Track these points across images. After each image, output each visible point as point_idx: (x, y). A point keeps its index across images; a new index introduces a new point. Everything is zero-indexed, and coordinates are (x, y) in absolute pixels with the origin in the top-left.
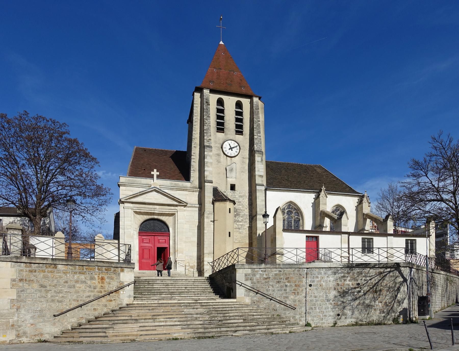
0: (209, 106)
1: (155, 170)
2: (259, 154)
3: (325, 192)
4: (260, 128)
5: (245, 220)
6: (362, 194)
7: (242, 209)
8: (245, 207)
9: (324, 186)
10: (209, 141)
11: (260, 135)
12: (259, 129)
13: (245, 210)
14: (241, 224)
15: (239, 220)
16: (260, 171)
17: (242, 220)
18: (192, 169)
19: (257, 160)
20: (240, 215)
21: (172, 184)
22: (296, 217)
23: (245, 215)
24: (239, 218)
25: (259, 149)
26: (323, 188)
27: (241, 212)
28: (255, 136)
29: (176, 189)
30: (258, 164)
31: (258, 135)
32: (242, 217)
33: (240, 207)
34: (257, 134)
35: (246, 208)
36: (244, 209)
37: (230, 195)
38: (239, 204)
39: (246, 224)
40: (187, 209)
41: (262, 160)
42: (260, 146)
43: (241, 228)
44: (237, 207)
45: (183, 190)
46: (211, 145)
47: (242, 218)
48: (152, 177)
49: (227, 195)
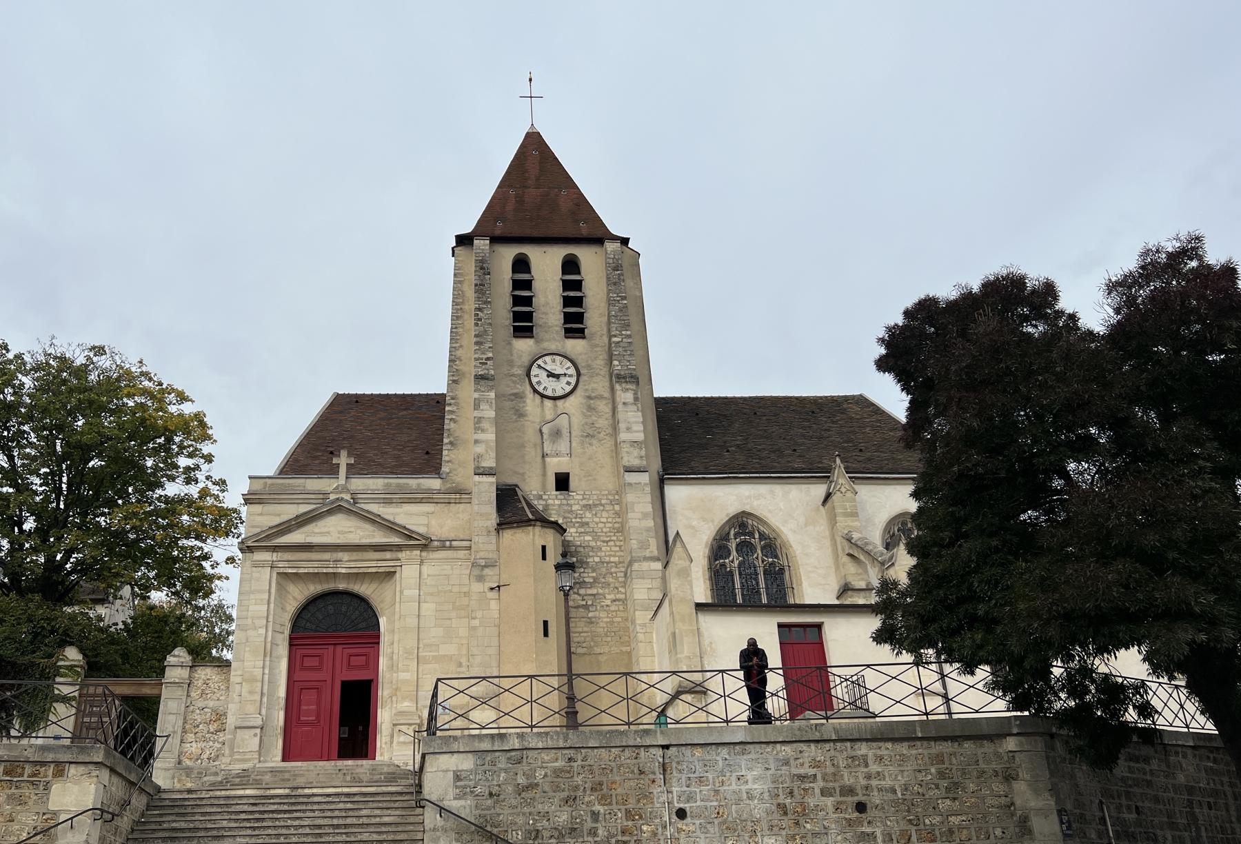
1: (344, 453)
2: (626, 382)
3: (847, 475)
5: (603, 580)
8: (602, 538)
11: (629, 333)
13: (603, 549)
14: (594, 591)
15: (587, 580)
17: (596, 580)
19: (623, 400)
20: (587, 563)
21: (388, 485)
22: (770, 560)
23: (603, 563)
24: (586, 575)
27: (591, 554)
28: (615, 336)
29: (400, 498)
30: (627, 411)
32: (594, 571)
33: (588, 538)
34: (620, 331)
35: (604, 542)
36: (599, 543)
37: (554, 505)
38: (583, 530)
39: (607, 591)
40: (431, 557)
41: (636, 399)
42: (629, 361)
43: (592, 605)
44: (576, 539)
45: (421, 501)
46: (492, 372)
47: (594, 574)
48: (333, 471)
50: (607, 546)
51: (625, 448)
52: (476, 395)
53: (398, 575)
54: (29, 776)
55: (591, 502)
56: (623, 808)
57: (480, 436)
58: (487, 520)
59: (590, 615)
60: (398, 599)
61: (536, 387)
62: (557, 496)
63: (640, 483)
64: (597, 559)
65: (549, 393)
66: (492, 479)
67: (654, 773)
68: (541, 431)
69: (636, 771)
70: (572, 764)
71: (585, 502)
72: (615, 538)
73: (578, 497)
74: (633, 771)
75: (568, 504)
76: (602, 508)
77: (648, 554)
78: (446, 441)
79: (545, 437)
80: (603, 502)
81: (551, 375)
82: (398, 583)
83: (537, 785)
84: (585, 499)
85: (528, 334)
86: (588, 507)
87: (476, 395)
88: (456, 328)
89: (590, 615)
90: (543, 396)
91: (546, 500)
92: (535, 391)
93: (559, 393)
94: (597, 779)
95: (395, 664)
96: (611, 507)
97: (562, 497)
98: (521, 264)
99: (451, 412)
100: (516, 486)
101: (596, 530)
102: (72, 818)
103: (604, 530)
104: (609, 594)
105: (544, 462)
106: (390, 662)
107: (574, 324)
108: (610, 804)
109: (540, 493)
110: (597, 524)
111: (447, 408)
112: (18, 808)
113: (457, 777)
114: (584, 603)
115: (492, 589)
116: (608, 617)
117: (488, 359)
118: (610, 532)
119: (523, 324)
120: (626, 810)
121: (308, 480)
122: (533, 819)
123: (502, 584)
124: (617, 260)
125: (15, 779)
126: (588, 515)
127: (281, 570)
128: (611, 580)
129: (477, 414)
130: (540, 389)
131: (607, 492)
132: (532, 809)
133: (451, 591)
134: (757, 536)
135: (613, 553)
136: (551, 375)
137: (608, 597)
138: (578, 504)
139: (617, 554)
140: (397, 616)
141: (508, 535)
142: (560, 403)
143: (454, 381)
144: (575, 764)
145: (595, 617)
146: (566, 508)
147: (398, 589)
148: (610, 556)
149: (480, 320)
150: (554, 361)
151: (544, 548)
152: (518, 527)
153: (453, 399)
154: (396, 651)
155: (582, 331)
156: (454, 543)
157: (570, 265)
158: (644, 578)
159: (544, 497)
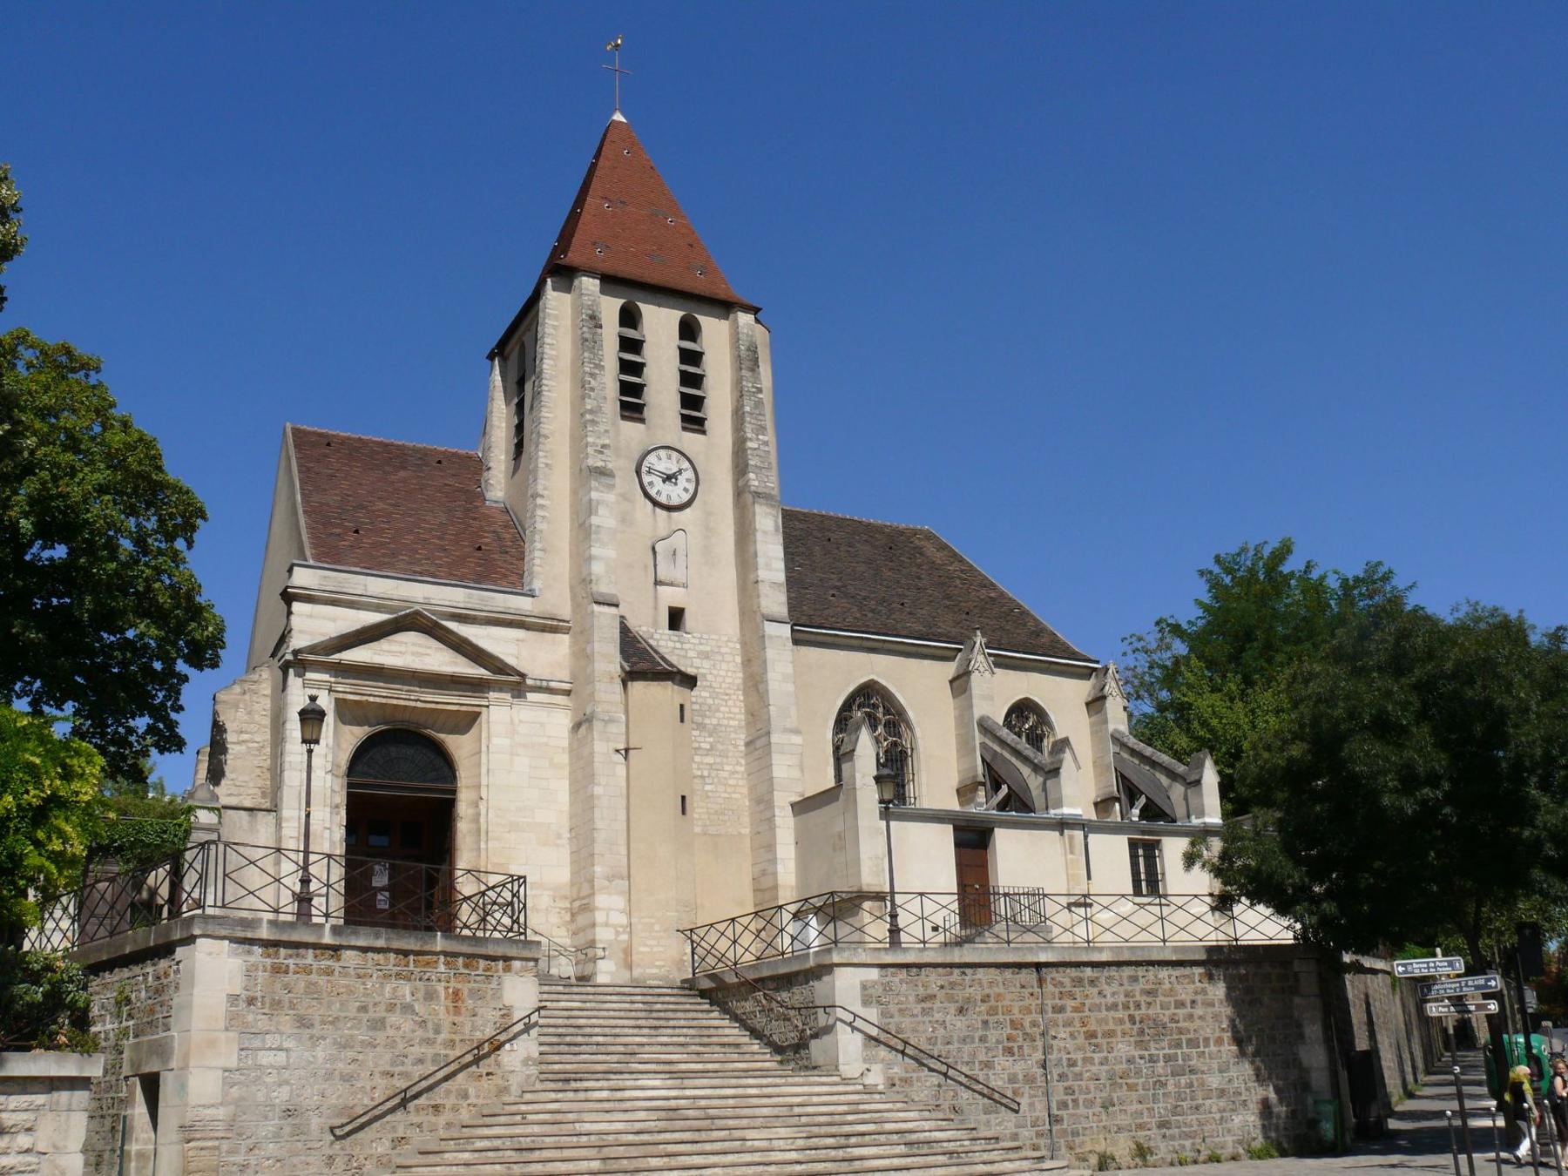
0: (599, 330)
4: (764, 415)
6: (1098, 662)
7: (710, 701)
9: (978, 633)
10: (602, 453)
11: (766, 438)
12: (760, 417)
13: (722, 709)
14: (710, 760)
15: (703, 745)
16: (774, 566)
18: (538, 545)
23: (721, 725)
25: (766, 487)
26: (979, 639)
28: (751, 440)
31: (758, 439)
35: (723, 700)
37: (667, 647)
41: (777, 530)
42: (767, 476)
46: (610, 466)
47: (711, 740)
49: (658, 646)
50: (726, 706)
51: (764, 589)
53: (484, 717)
54: (484, 971)
55: (708, 648)
56: (1008, 1018)
58: (609, 662)
59: (708, 788)
60: (484, 748)
64: (714, 721)
65: (663, 499)
66: (613, 610)
67: (1033, 987)
68: (653, 548)
69: (1018, 985)
70: (963, 977)
71: (701, 648)
72: (735, 697)
73: (697, 641)
74: (1015, 986)
75: (682, 649)
76: (720, 658)
77: (788, 726)
79: (658, 557)
80: (724, 650)
81: (669, 478)
82: (484, 726)
83: (935, 996)
84: (701, 644)
85: (636, 415)
86: (705, 656)
88: (549, 391)
89: (708, 788)
90: (656, 503)
91: (658, 640)
92: (647, 495)
93: (675, 501)
94: (987, 991)
95: (483, 828)
96: (731, 658)
97: (676, 639)
98: (629, 317)
99: (542, 506)
101: (714, 685)
102: (529, 1016)
103: (723, 685)
104: (727, 764)
105: (656, 590)
106: (473, 826)
107: (693, 413)
108: (997, 1014)
110: (715, 676)
112: (479, 1002)
113: (864, 987)
114: (699, 773)
115: (618, 751)
116: (725, 792)
117: (604, 446)
118: (729, 688)
119: (632, 403)
120: (1012, 1021)
121: (369, 578)
122: (933, 1027)
123: (632, 747)
124: (752, 336)
125: (473, 973)
126: (706, 664)
127: (341, 696)
128: (730, 747)
130: (653, 492)
132: (931, 1019)
133: (547, 745)
134: (881, 709)
135: (732, 716)
136: (669, 478)
137: (727, 768)
138: (694, 650)
139: (738, 716)
140: (484, 770)
141: (637, 687)
142: (675, 515)
144: (967, 978)
145: (712, 791)
146: (683, 653)
147: (484, 735)
148: (730, 718)
151: (682, 706)
152: (652, 680)
153: (545, 489)
154: (483, 812)
156: (553, 685)
157: (689, 330)
158: (782, 753)
159: (656, 636)
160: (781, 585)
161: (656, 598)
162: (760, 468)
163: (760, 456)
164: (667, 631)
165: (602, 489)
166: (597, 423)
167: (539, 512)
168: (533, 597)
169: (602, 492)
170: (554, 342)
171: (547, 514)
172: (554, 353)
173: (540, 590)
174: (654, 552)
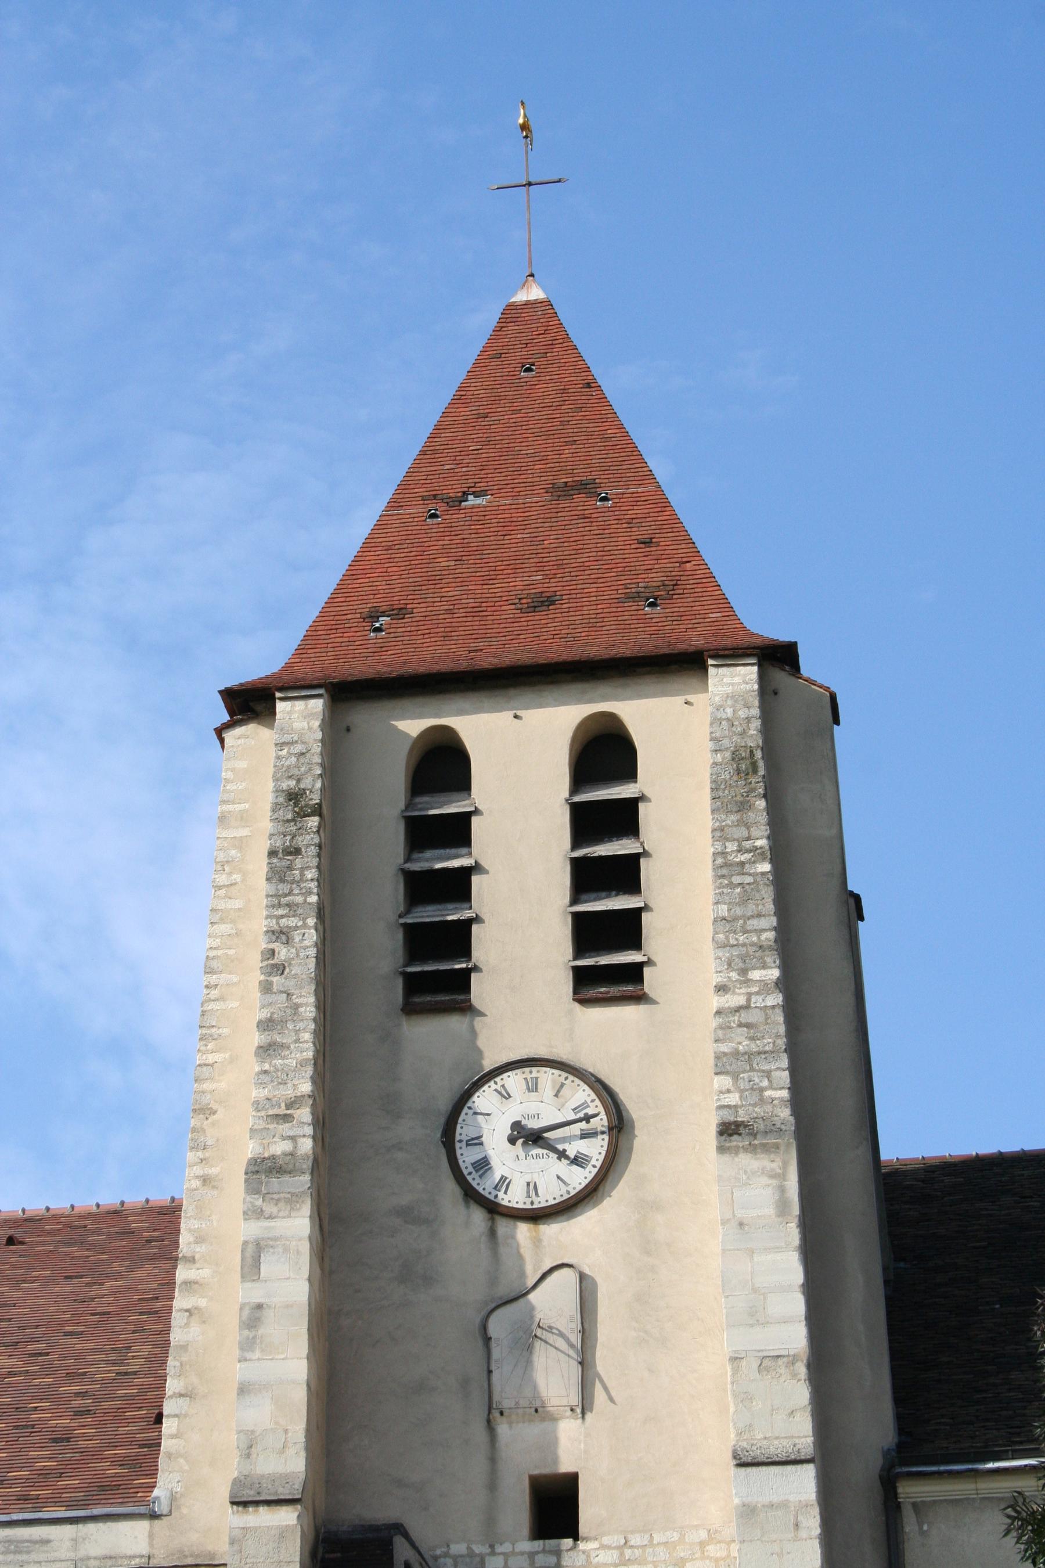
31: (748, 982)
34: (744, 972)
52: (254, 1229)
57: (255, 1370)
61: (474, 1180)
62: (532, 1555)
63: (784, 1505)
78: (172, 1385)
79: (496, 1353)
87: (254, 1229)
93: (550, 1195)
100: (399, 1529)
109: (478, 1549)
111: (182, 1274)
129: (255, 1293)
131: (703, 1535)
143: (206, 1180)
149: (280, 969)
150: (533, 1087)
153: (200, 1240)
155: (634, 973)
160: (794, 1359)
161: (493, 1459)
162: (749, 1055)
163: (748, 1026)
164: (526, 1545)
165: (270, 1209)
166: (283, 1046)
167: (180, 1302)
168: (154, 1516)
169: (271, 1217)
170: (237, 877)
171: (202, 1303)
172: (237, 904)
173: (173, 1498)
174: (487, 1340)
